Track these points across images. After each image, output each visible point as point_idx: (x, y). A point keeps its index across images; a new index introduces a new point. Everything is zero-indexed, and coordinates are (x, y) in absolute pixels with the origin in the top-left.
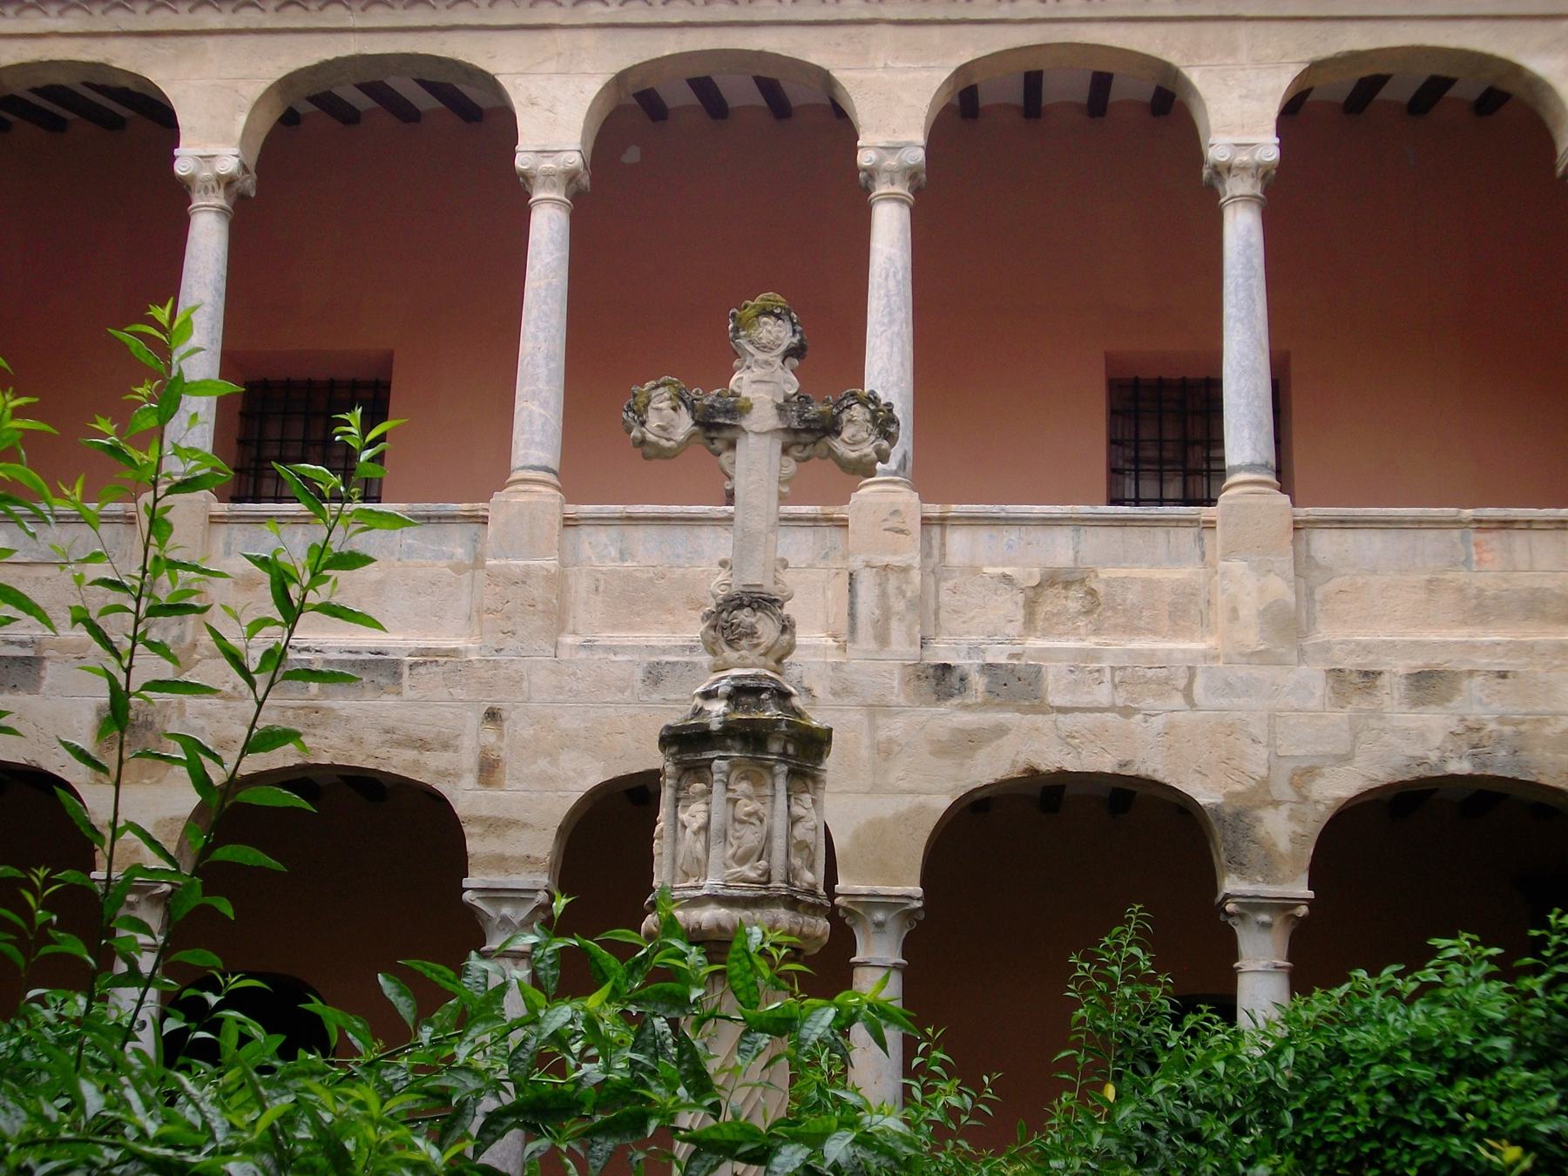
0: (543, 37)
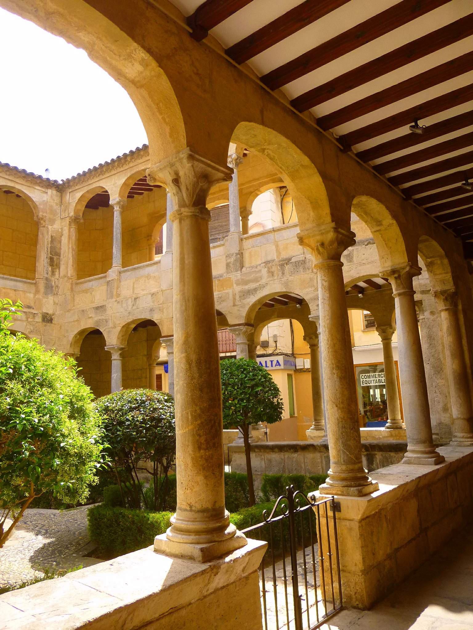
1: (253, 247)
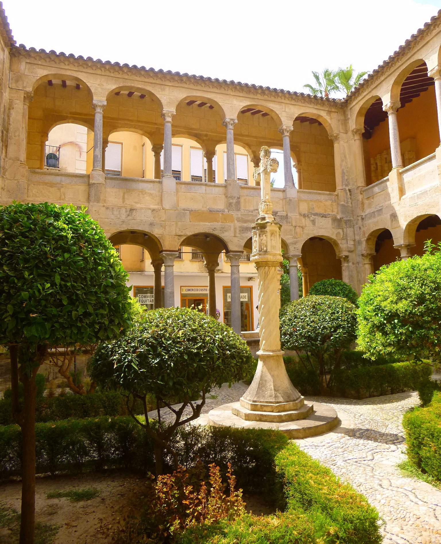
0: (428, 45)
1: (247, 196)
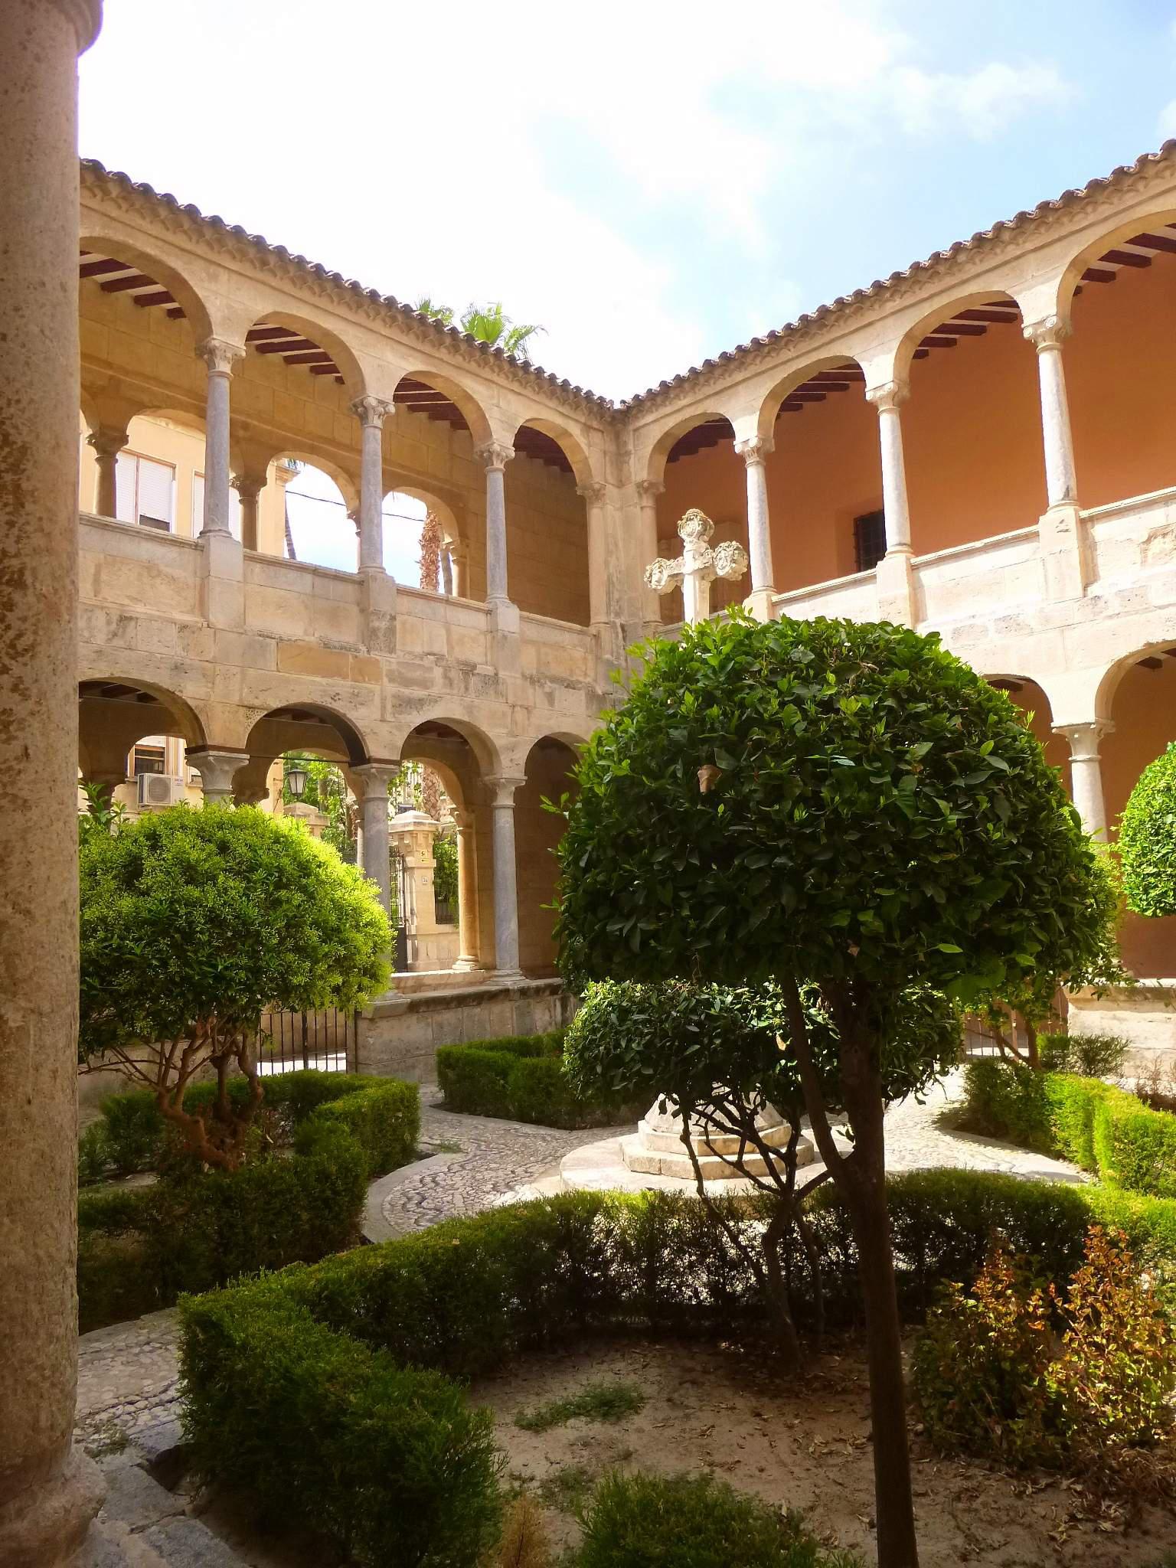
0: (870, 330)
1: (409, 614)
